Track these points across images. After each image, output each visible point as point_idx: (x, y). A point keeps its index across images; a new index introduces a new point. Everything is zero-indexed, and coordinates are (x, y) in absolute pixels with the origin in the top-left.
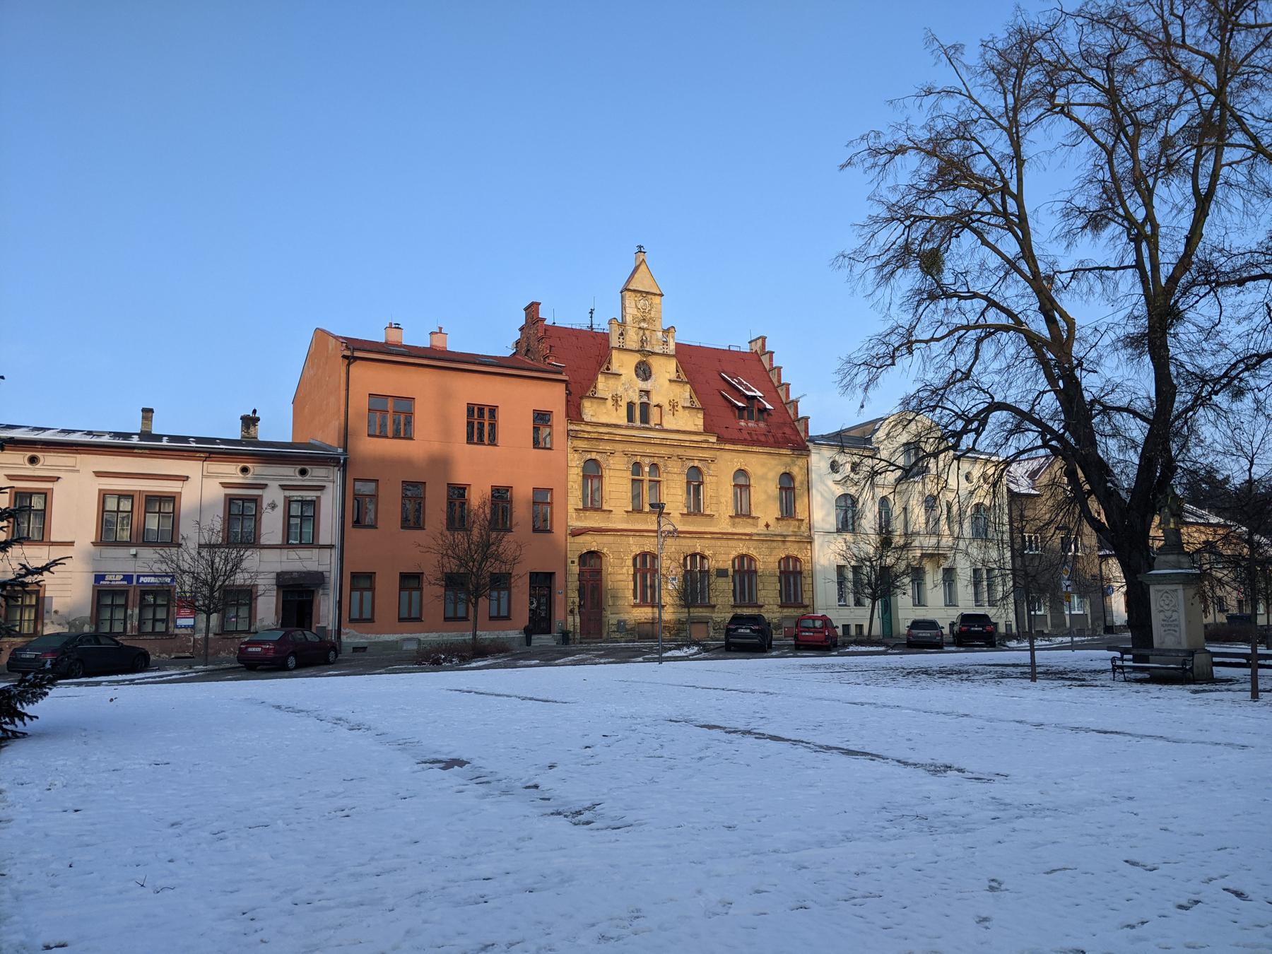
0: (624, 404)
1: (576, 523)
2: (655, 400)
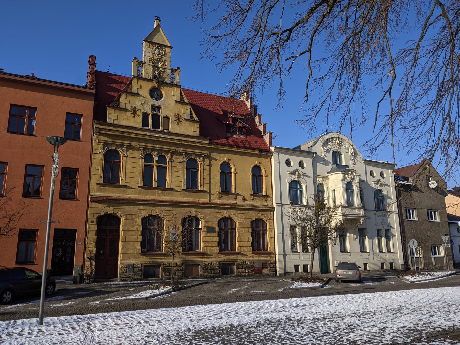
2: (163, 113)
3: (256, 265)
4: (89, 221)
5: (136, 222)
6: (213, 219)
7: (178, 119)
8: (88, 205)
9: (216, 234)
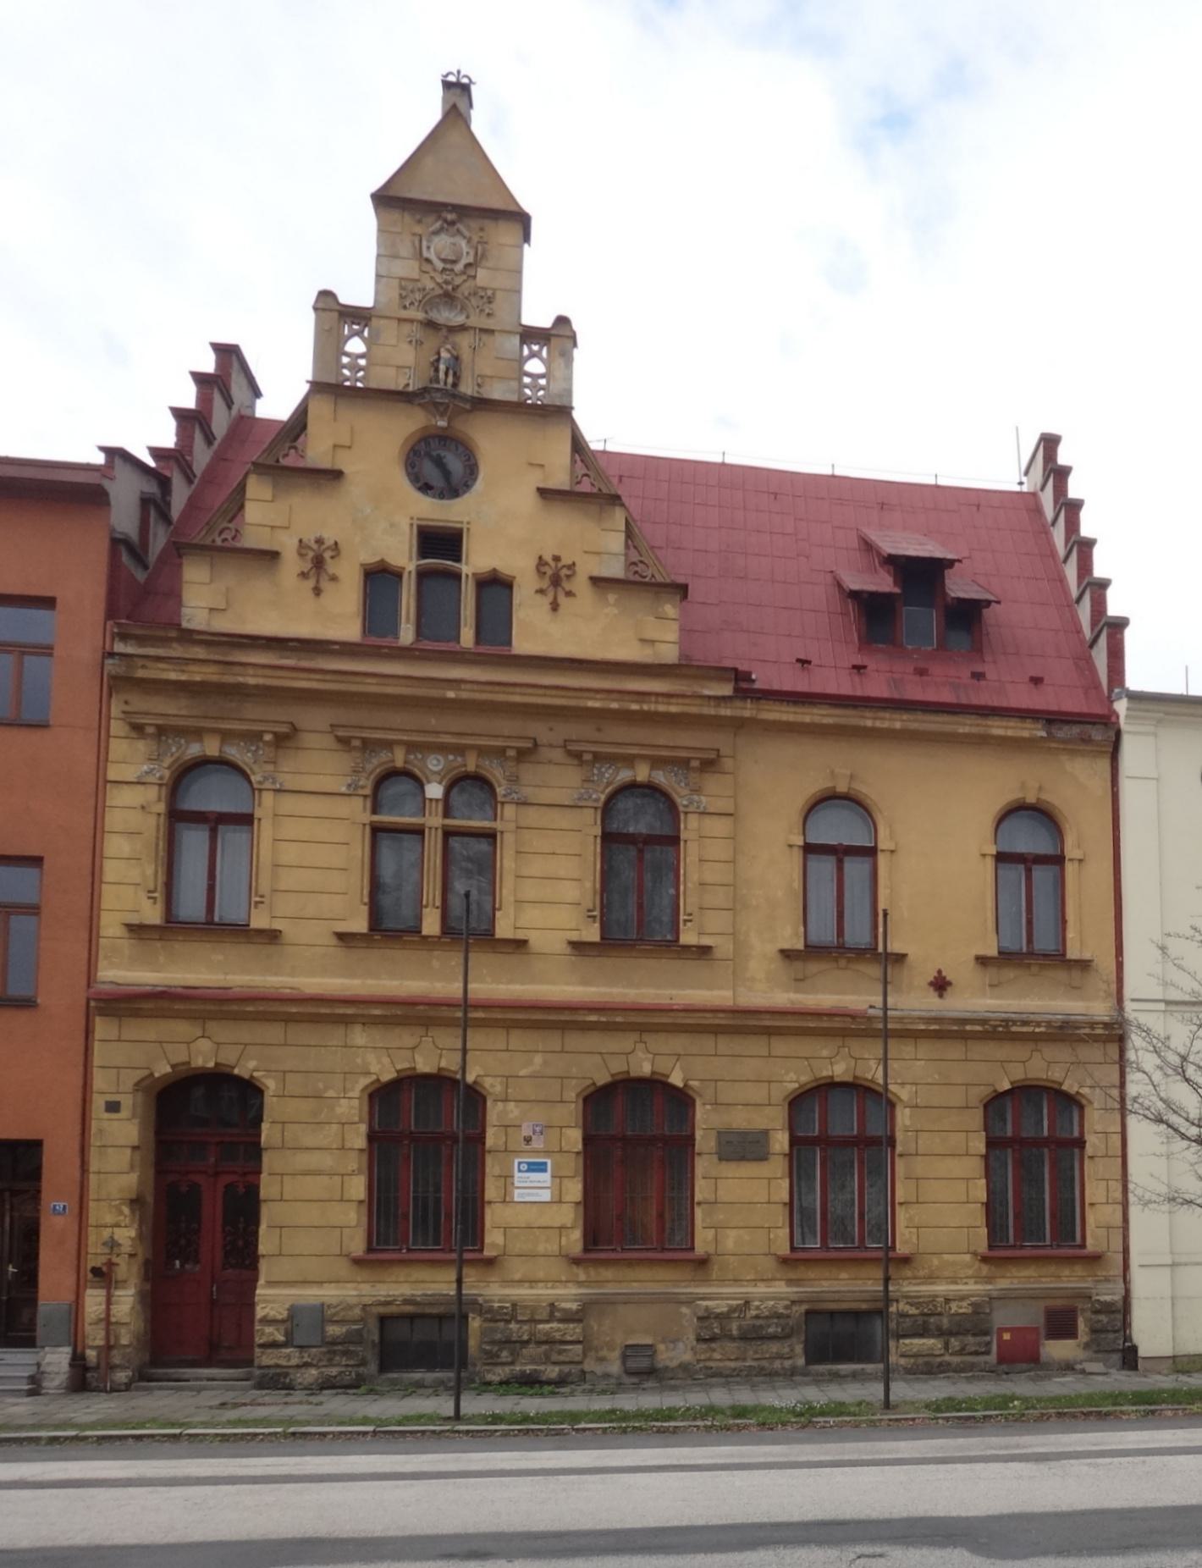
1: (123, 970)
2: (477, 559)
6: (757, 1093)
7: (556, 581)
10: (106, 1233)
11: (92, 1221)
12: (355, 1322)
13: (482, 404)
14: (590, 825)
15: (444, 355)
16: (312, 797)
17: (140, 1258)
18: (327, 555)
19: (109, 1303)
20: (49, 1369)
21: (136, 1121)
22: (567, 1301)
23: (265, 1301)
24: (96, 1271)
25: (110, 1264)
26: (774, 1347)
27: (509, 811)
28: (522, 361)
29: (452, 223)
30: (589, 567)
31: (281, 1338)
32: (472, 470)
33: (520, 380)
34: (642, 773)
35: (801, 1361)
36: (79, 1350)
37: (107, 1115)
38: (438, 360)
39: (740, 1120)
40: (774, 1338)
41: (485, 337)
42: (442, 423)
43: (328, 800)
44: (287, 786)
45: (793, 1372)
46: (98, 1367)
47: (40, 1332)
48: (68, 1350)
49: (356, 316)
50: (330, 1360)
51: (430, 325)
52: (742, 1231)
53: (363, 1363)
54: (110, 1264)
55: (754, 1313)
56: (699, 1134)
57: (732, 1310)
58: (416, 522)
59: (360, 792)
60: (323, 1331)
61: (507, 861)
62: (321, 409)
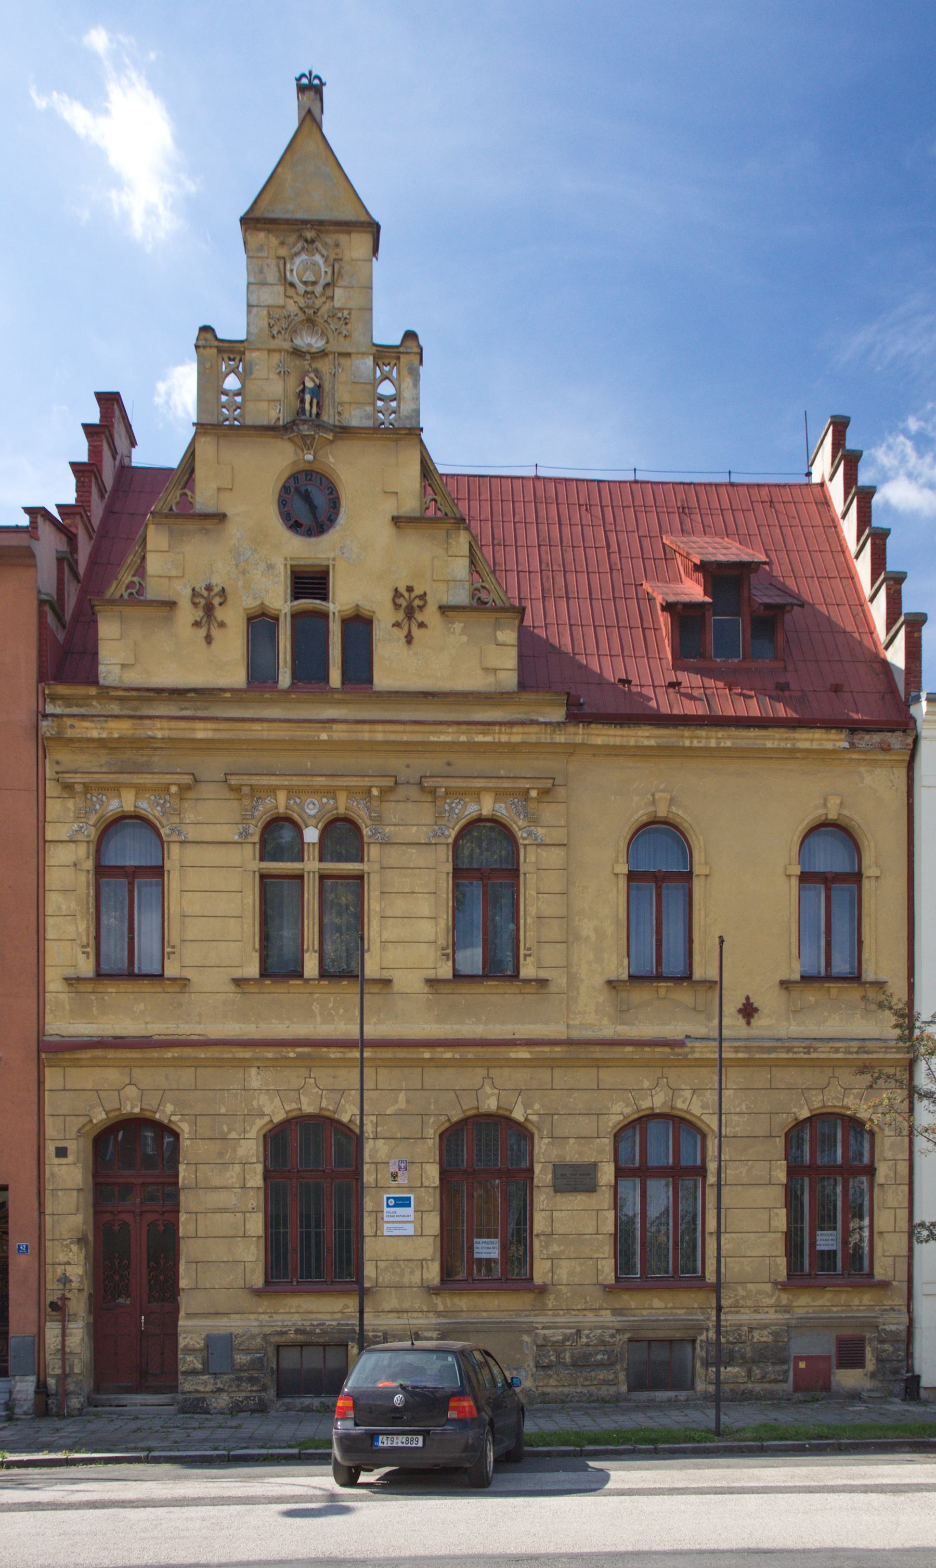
0: (233, 618)
2: (343, 598)
3: (800, 1346)
4: (50, 1149)
5: (234, 1150)
6: (586, 1125)
7: (410, 613)
8: (40, 1082)
9: (604, 1198)
10: (60, 1270)
11: (49, 1260)
12: (258, 1351)
13: (344, 432)
14: (441, 862)
15: (309, 384)
16: (210, 847)
17: (86, 1294)
18: (216, 601)
19: (64, 1335)
20: (19, 1396)
21: (80, 1165)
22: (428, 1330)
23: (185, 1332)
24: (54, 1306)
25: (64, 1298)
26: (602, 1375)
27: (373, 852)
28: (376, 383)
29: (313, 241)
30: (439, 595)
31: (199, 1366)
32: (335, 504)
33: (374, 404)
34: (487, 806)
35: (624, 1388)
36: (42, 1378)
37: (57, 1161)
38: (303, 391)
39: (572, 1153)
40: (601, 1365)
41: (344, 362)
42: (310, 457)
43: (222, 850)
44: (190, 838)
45: (617, 1399)
46: (56, 1395)
47: (11, 1363)
48: (33, 1378)
49: (231, 351)
50: (238, 1386)
51: (297, 353)
52: (573, 1263)
53: (264, 1388)
54: (64, 1298)
55: (584, 1340)
56: (537, 1168)
57: (566, 1338)
58: (289, 563)
59: (250, 839)
60: (232, 1358)
61: (373, 905)
62: (206, 449)
